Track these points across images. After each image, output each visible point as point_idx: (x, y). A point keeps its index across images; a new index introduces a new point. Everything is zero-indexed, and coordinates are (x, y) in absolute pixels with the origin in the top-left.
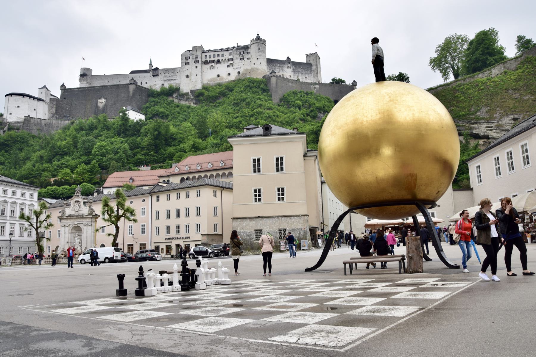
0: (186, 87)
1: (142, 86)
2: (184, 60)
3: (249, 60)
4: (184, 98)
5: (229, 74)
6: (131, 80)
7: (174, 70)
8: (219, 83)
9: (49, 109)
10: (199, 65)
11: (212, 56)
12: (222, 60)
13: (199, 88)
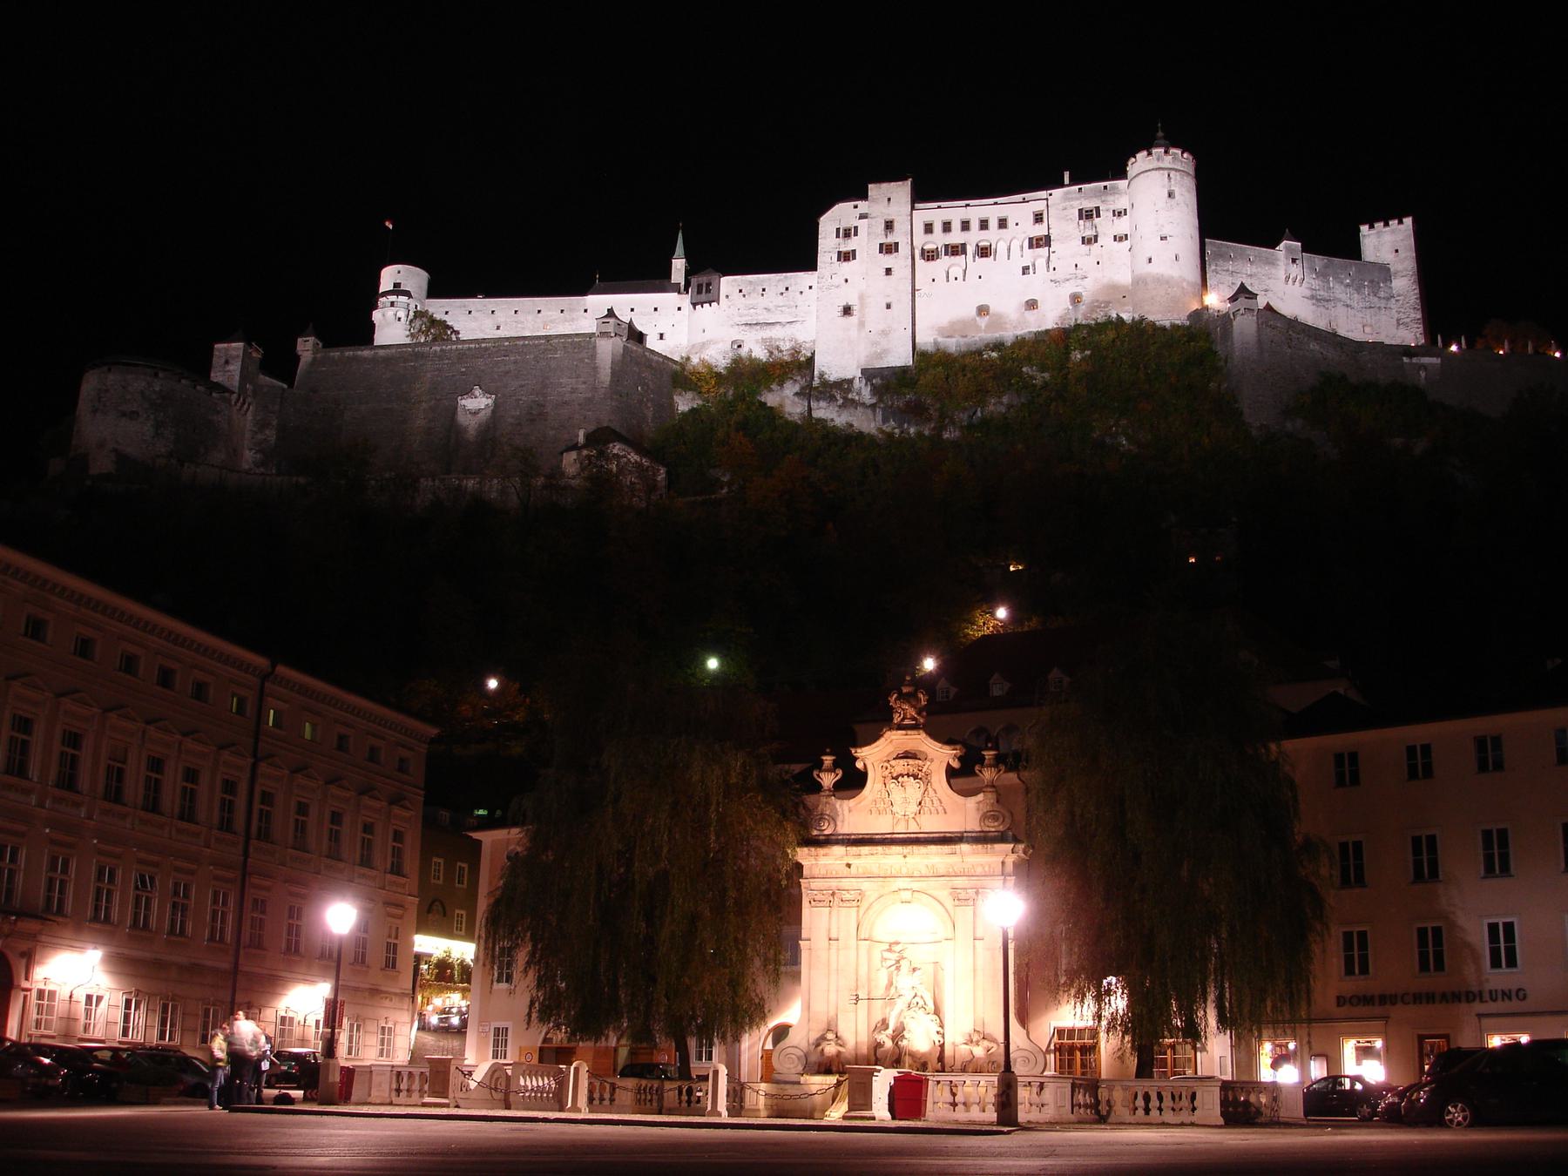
3: (1126, 244)
10: (899, 261)
11: (956, 226)
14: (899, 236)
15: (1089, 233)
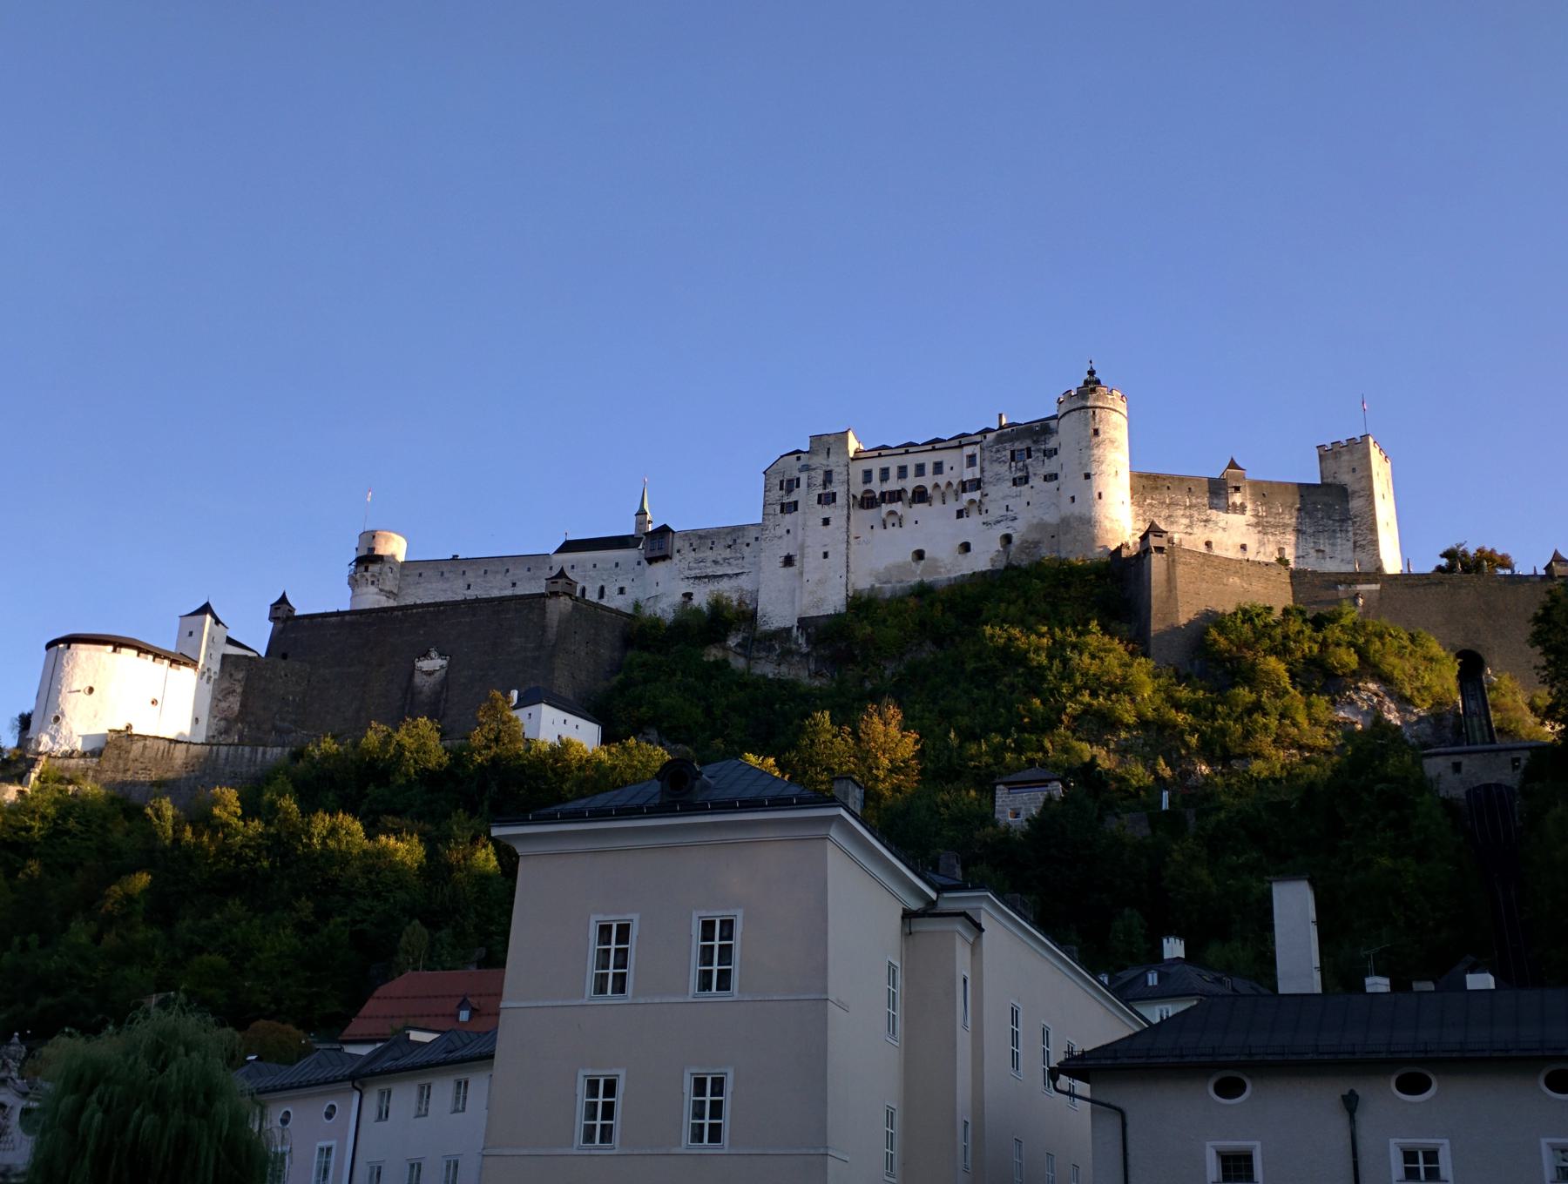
0: (781, 604)
1: (604, 602)
2: (776, 494)
3: (1054, 484)
4: (771, 649)
5: (966, 547)
6: (553, 580)
7: (733, 536)
8: (921, 584)
9: (214, 698)
10: (836, 513)
11: (893, 472)
12: (937, 486)
13: (829, 610)
14: (838, 488)
15: (1020, 474)
